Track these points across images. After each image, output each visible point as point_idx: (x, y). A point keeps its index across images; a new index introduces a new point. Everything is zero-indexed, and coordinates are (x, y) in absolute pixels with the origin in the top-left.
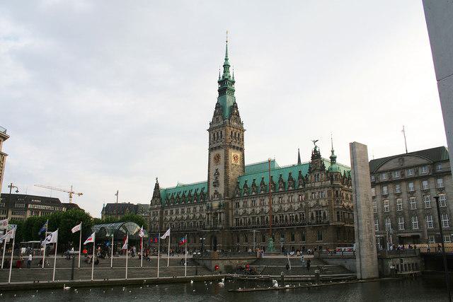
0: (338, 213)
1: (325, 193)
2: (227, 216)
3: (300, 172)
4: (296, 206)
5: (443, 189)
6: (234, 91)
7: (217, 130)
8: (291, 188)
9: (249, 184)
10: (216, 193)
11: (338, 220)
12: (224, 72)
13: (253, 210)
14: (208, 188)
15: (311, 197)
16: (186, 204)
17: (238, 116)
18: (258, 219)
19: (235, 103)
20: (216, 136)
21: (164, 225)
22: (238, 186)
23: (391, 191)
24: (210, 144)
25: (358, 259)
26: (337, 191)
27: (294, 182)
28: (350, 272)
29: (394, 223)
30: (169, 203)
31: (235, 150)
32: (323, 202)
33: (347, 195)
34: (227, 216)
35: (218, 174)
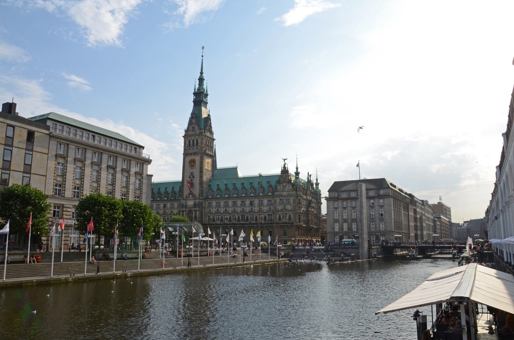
0: (299, 216)
4: (265, 209)
5: (383, 206)
7: (193, 138)
9: (223, 188)
10: (191, 193)
11: (300, 221)
12: (199, 85)
13: (226, 210)
15: (279, 203)
19: (209, 115)
20: (191, 143)
23: (349, 204)
24: (185, 150)
26: (299, 200)
27: (264, 189)
29: (350, 226)
32: (289, 207)
34: (201, 214)
35: (193, 177)
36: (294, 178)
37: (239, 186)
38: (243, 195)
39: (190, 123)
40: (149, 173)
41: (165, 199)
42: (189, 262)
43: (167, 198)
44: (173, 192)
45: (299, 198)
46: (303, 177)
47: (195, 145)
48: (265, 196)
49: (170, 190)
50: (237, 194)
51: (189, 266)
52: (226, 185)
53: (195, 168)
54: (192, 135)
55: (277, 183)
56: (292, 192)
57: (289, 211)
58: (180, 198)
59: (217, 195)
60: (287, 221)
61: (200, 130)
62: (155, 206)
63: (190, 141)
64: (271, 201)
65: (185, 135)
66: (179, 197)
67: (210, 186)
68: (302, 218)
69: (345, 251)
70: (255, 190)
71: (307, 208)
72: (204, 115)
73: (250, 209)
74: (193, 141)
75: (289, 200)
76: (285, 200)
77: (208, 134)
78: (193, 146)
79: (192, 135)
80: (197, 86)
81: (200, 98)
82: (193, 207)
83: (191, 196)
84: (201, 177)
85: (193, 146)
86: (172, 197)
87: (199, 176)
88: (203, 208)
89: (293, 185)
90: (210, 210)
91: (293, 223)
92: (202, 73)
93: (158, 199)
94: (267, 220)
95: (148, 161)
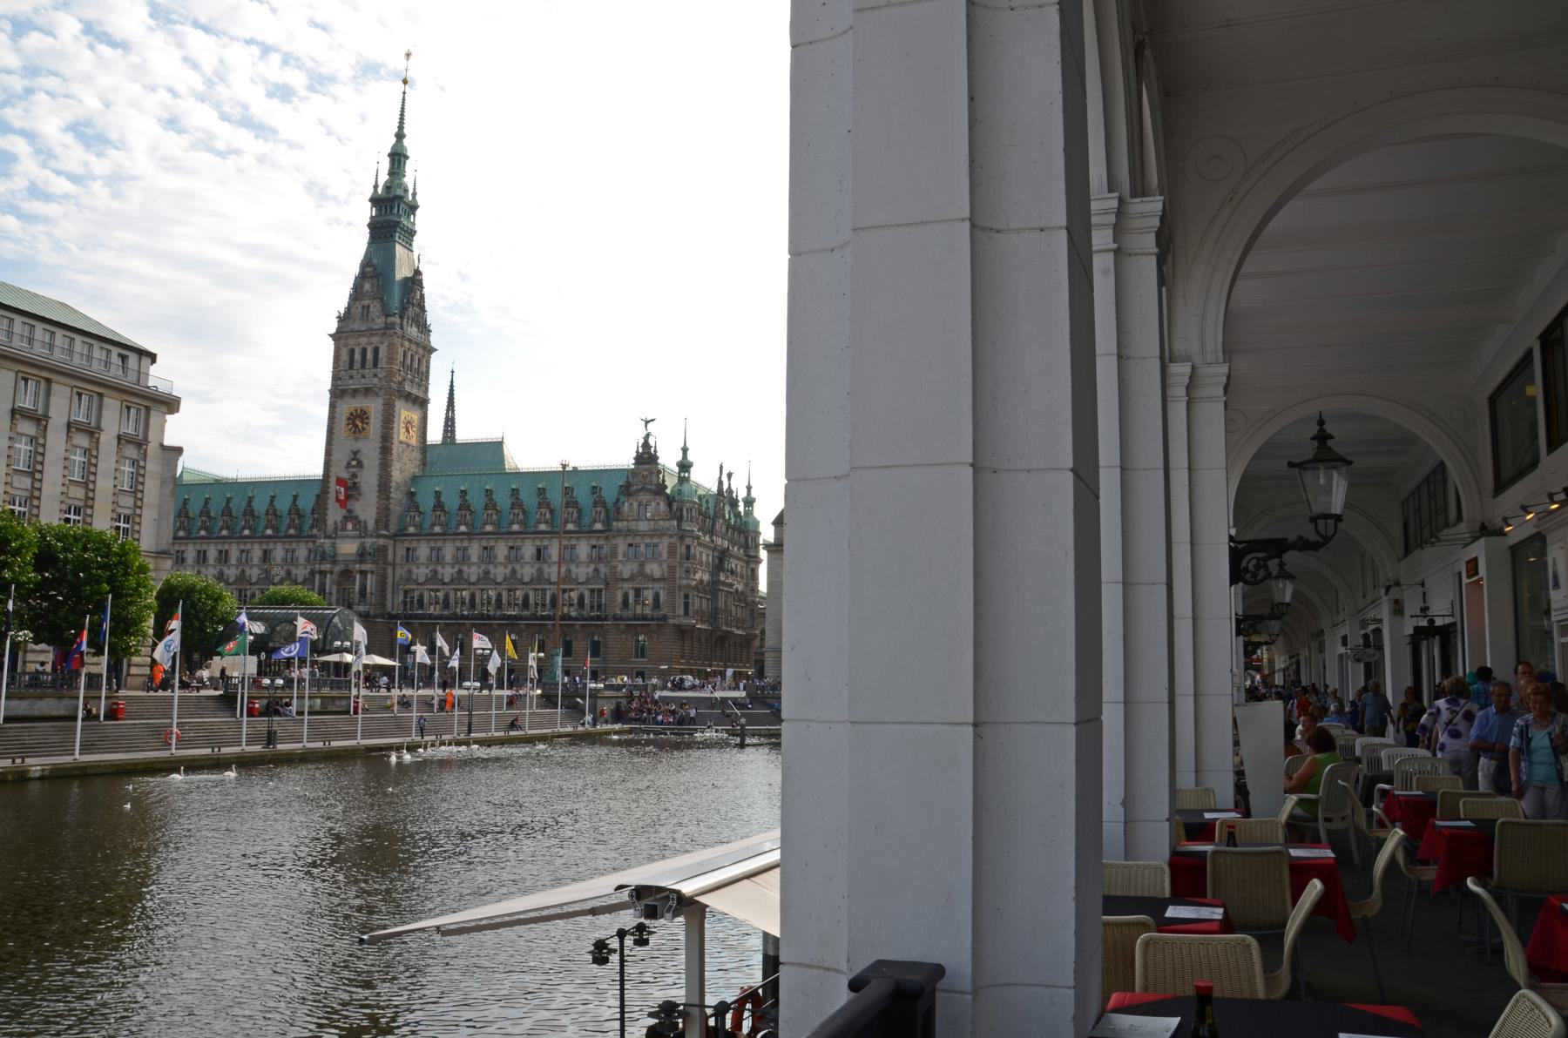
0: (686, 596)
1: (664, 545)
2: (382, 584)
4: (582, 572)
6: (412, 233)
7: (363, 340)
9: (452, 502)
11: (686, 613)
13: (460, 571)
17: (423, 309)
20: (357, 357)
26: (688, 547)
27: (580, 511)
31: (410, 405)
32: (654, 569)
34: (382, 584)
35: (360, 465)
36: (676, 480)
37: (503, 500)
38: (516, 527)
39: (357, 293)
40: (167, 442)
41: (269, 532)
42: (269, 733)
44: (295, 511)
45: (688, 541)
46: (704, 478)
47: (369, 363)
48: (584, 532)
49: (283, 505)
50: (497, 524)
51: (269, 743)
52: (464, 493)
53: (366, 437)
54: (360, 333)
55: (620, 493)
56: (667, 524)
57: (655, 580)
58: (315, 531)
59: (433, 525)
60: (648, 611)
61: (387, 316)
62: (190, 553)
63: (352, 352)
64: (601, 547)
65: (339, 331)
66: (312, 527)
67: (413, 494)
68: (696, 603)
70: (552, 512)
71: (712, 575)
72: (402, 272)
73: (534, 571)
74: (364, 351)
75: (656, 545)
76: (642, 548)
77: (413, 331)
78: (363, 365)
79: (360, 333)
80: (384, 178)
81: (391, 215)
82: (355, 562)
83: (350, 526)
84: (385, 466)
85: (363, 365)
86: (289, 527)
87: (377, 463)
88: (386, 563)
89: (670, 501)
91: (665, 618)
92: (400, 136)
93: (247, 532)
94: (587, 607)
95: (171, 404)
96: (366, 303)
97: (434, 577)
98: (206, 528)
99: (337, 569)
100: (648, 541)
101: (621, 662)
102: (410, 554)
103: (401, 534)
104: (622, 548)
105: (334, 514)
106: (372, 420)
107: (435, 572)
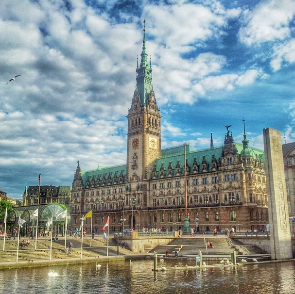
2: (145, 198)
3: (213, 156)
7: (136, 116)
8: (204, 171)
13: (170, 191)
14: (127, 171)
16: (106, 186)
18: (174, 199)
20: (134, 122)
21: (85, 206)
22: (155, 170)
25: (272, 240)
28: (266, 252)
30: (90, 186)
33: (259, 177)
34: (145, 198)
35: (137, 157)
43: (117, 182)
47: (138, 124)
48: (210, 172)
53: (138, 148)
54: (134, 114)
56: (239, 166)
61: (142, 107)
69: (257, 243)
75: (235, 175)
76: (230, 176)
90: (154, 192)
91: (241, 204)
96: (136, 104)
97: (162, 194)
98: (99, 184)
99: (132, 193)
100: (232, 173)
101: (226, 223)
102: (155, 187)
103: (151, 179)
104: (223, 177)
105: (130, 175)
106: (139, 142)
107: (162, 192)
